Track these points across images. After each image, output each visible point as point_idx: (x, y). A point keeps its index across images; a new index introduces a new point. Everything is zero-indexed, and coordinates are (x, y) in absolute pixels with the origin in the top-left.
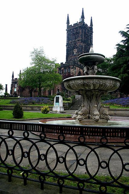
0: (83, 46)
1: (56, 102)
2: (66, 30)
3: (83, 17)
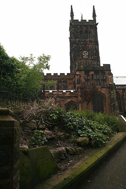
3: (94, 15)
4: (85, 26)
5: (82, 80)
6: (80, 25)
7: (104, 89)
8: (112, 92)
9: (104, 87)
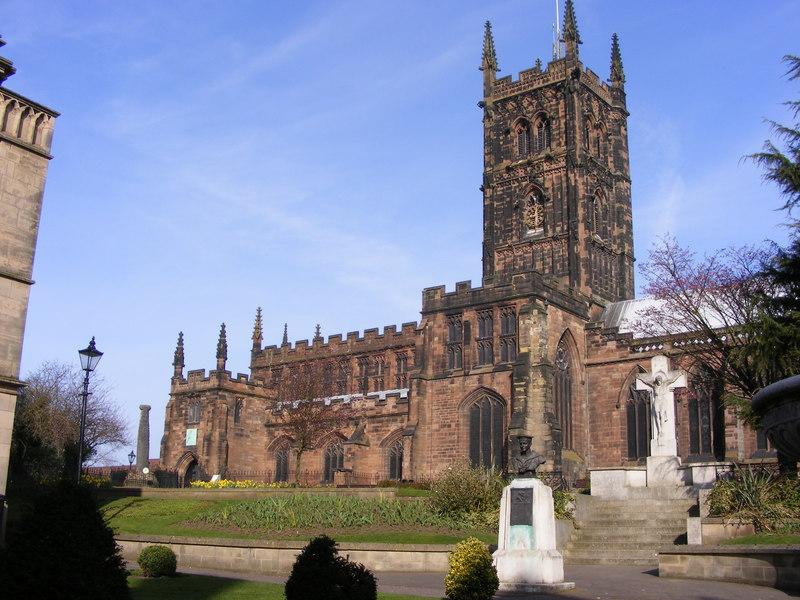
1: (513, 523)
2: (482, 105)
3: (571, 36)
4: (534, 94)
6: (514, 99)
8: (521, 386)
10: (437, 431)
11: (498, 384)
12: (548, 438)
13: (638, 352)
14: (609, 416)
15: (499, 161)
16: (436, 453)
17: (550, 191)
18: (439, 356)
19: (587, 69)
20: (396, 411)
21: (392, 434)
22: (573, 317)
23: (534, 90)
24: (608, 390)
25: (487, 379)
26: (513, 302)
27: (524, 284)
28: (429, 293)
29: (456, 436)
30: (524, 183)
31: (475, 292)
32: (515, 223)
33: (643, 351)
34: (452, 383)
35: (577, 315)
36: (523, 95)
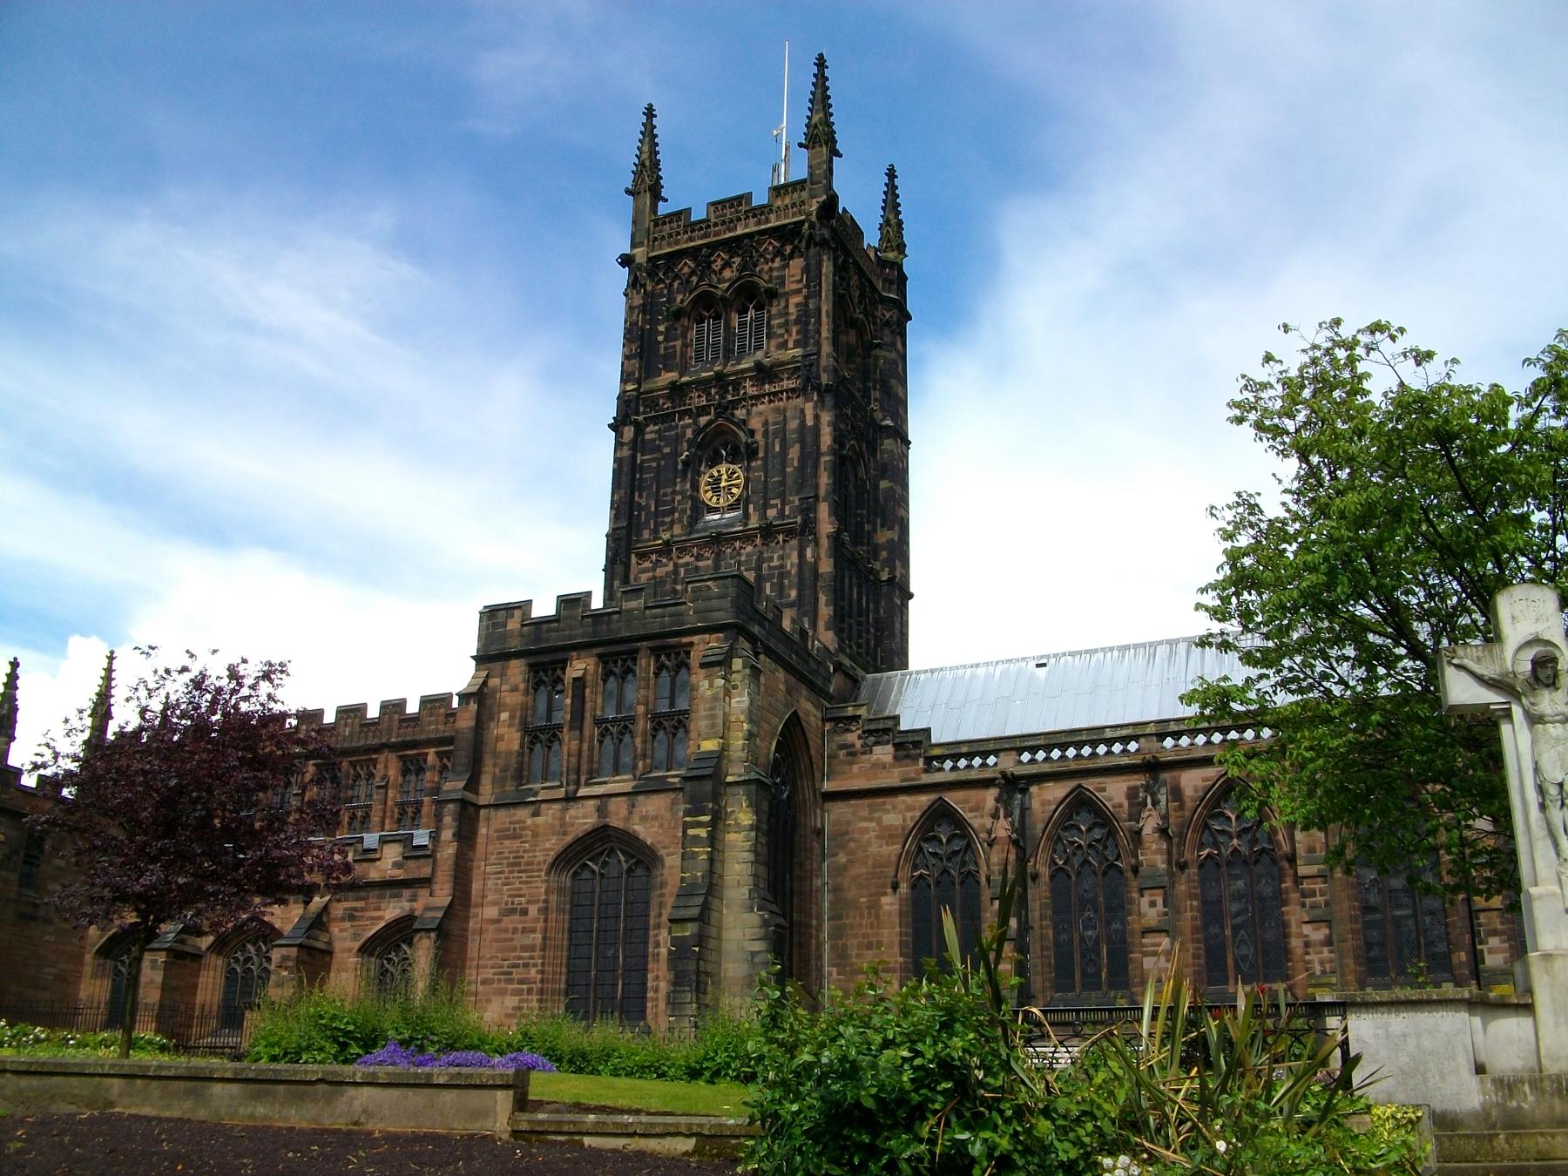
0: (816, 429)
2: (626, 261)
4: (733, 245)
5: (500, 738)
6: (693, 253)
7: (654, 805)
8: (700, 825)
9: (660, 788)
10: (498, 921)
11: (644, 819)
12: (758, 946)
13: (941, 769)
14: (874, 906)
15: (649, 371)
16: (489, 973)
17: (759, 437)
18: (509, 753)
19: (844, 209)
20: (400, 874)
21: (388, 926)
22: (804, 692)
23: (738, 239)
24: (874, 849)
25: (618, 808)
26: (685, 640)
27: (715, 603)
28: (493, 616)
29: (539, 936)
30: (703, 420)
31: (597, 616)
32: (678, 498)
33: (954, 768)
34: (536, 814)
35: (812, 686)
36: (713, 247)
